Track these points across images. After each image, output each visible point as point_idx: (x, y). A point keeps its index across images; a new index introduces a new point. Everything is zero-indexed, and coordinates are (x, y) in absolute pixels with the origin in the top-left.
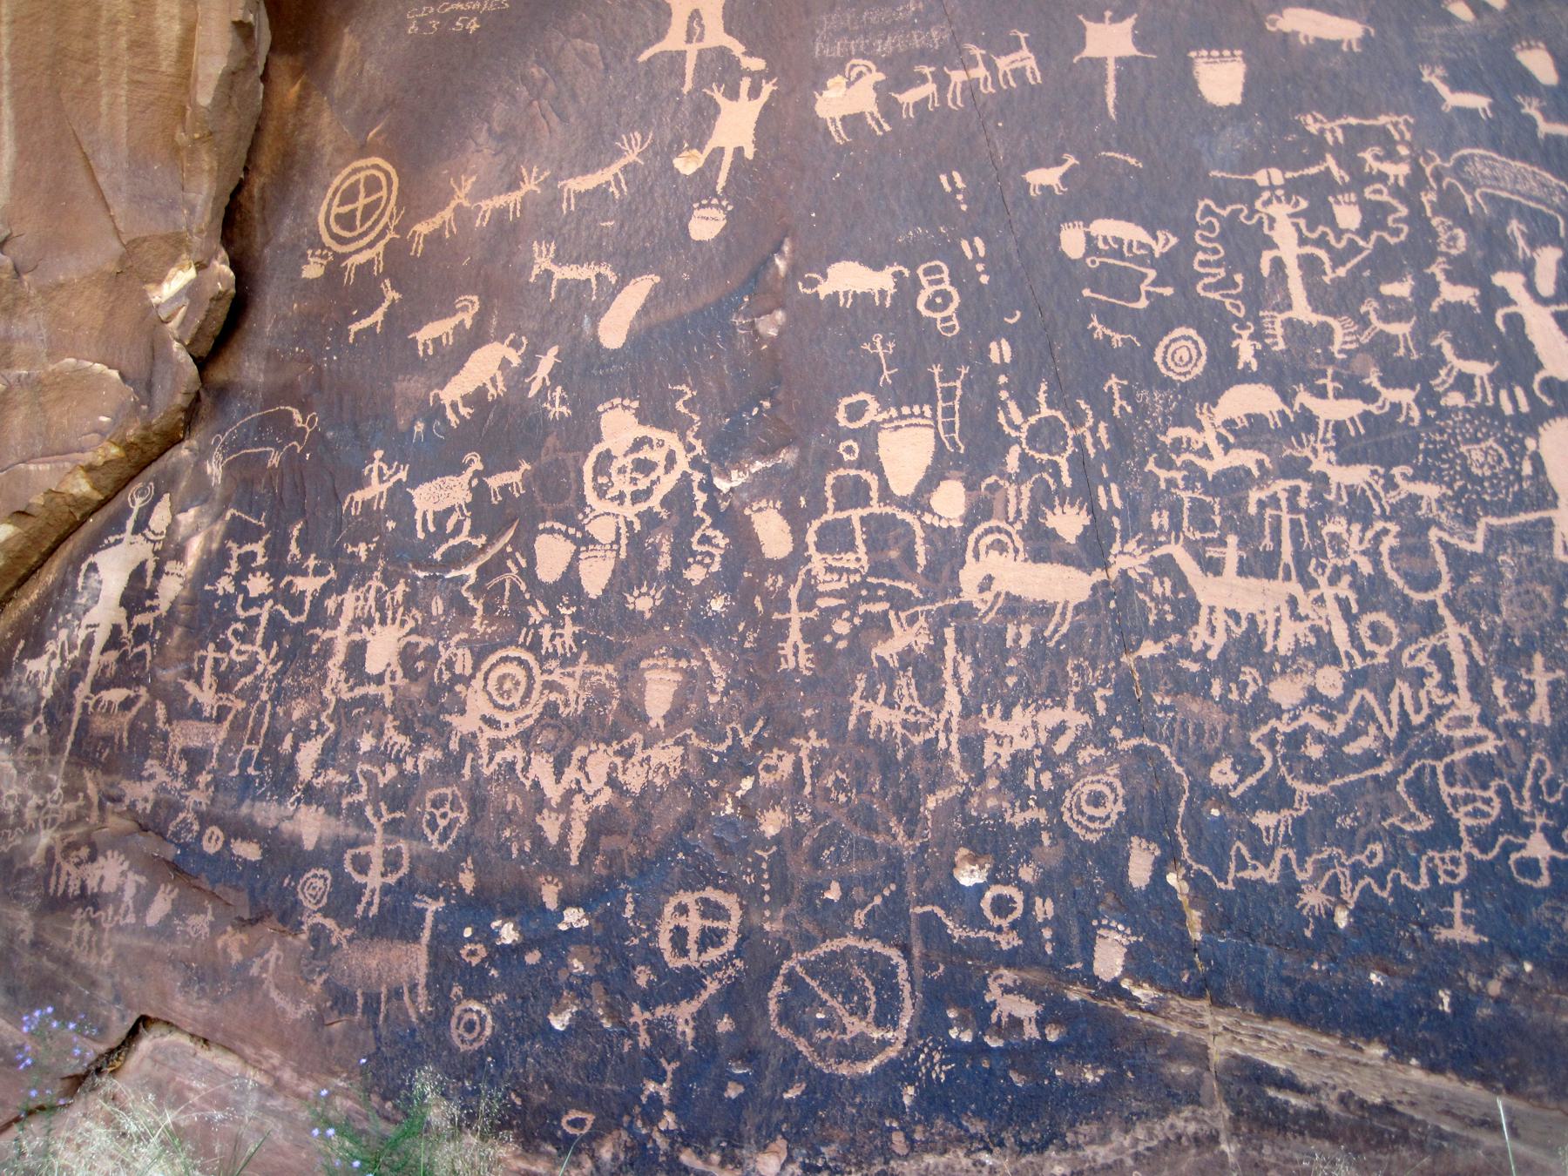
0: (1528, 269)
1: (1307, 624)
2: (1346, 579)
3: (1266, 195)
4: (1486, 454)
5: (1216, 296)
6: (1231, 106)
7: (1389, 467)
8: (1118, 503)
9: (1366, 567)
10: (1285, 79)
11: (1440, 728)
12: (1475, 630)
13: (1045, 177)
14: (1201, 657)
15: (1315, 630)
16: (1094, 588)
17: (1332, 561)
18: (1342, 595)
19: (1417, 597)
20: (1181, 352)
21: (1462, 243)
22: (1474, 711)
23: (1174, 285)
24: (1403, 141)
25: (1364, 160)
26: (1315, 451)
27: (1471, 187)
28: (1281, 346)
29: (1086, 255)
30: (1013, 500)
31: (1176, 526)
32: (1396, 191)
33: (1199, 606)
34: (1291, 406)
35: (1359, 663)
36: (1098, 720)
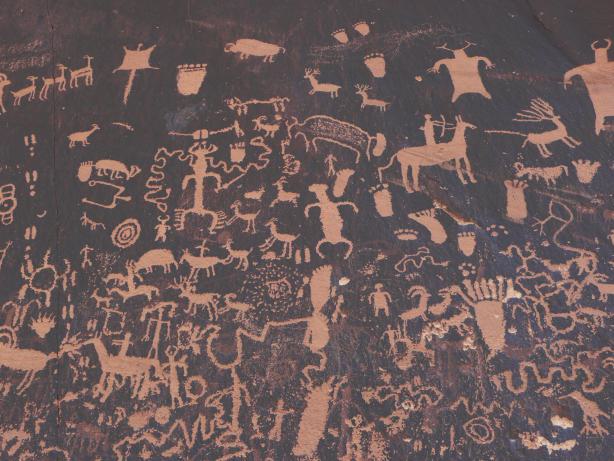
0: (330, 182)
1: (157, 382)
2: (185, 357)
3: (196, 144)
4: (280, 285)
5: (153, 201)
6: (192, 95)
7: (223, 294)
8: (72, 316)
9: (197, 350)
10: (227, 76)
11: (218, 443)
12: (249, 386)
13: (81, 137)
14: (96, 401)
15: (161, 386)
16: (48, 363)
17: (180, 346)
18: (180, 365)
19: (221, 367)
20: (127, 232)
21: (297, 169)
22: (240, 432)
23: (132, 196)
24: (280, 112)
25: (255, 123)
26: (185, 286)
27: (310, 138)
28: (182, 228)
29: (90, 180)
30: (17, 314)
31: (99, 328)
32: (268, 141)
33: (101, 372)
34: (178, 261)
35: (181, 404)
36: (34, 436)
